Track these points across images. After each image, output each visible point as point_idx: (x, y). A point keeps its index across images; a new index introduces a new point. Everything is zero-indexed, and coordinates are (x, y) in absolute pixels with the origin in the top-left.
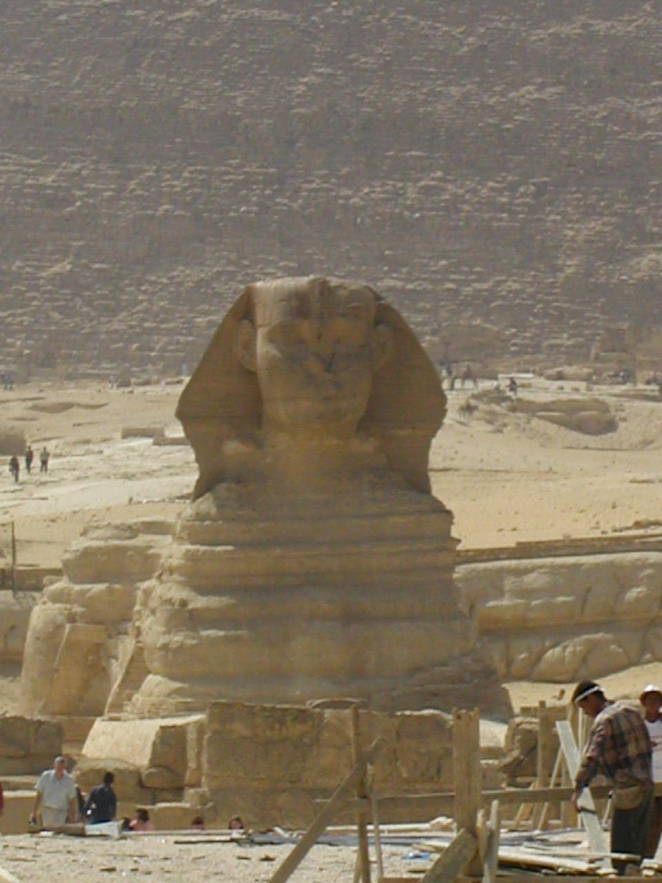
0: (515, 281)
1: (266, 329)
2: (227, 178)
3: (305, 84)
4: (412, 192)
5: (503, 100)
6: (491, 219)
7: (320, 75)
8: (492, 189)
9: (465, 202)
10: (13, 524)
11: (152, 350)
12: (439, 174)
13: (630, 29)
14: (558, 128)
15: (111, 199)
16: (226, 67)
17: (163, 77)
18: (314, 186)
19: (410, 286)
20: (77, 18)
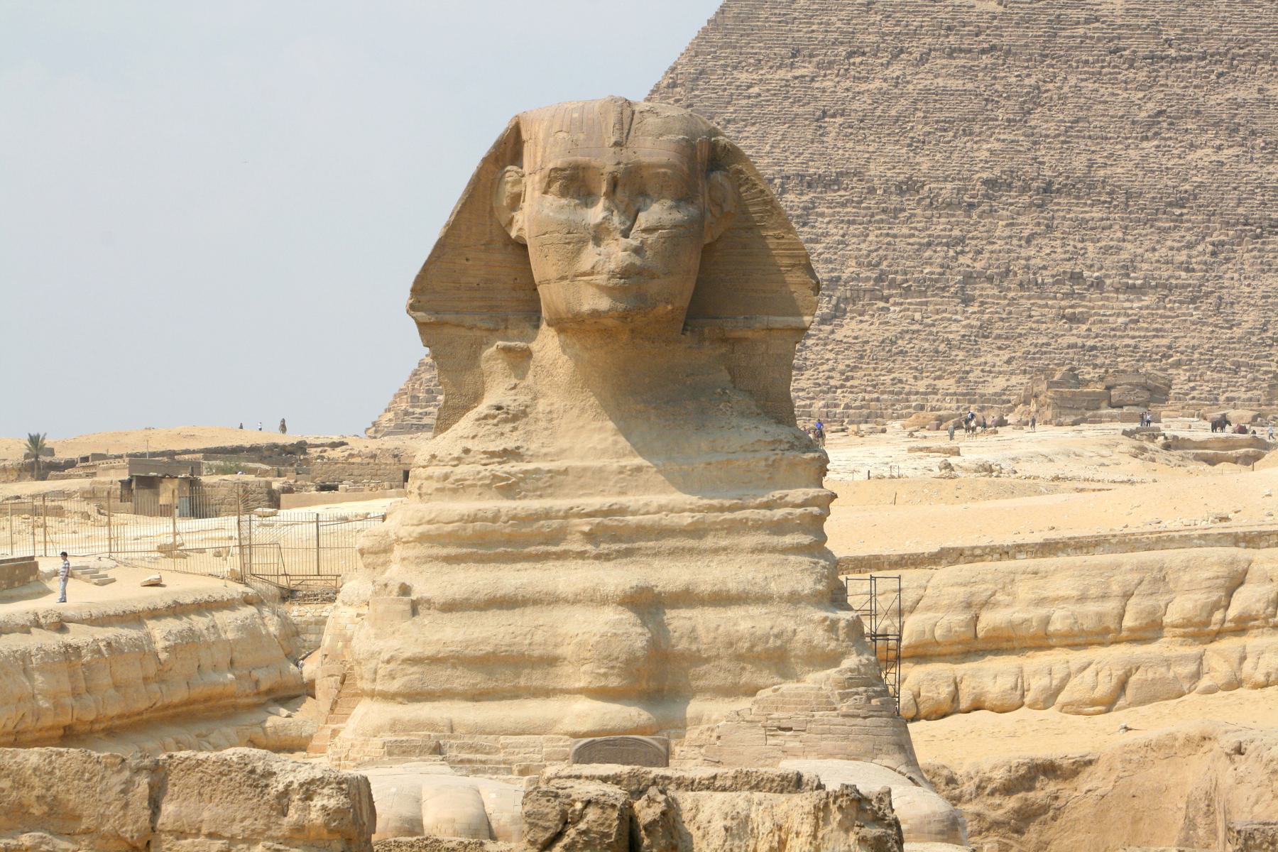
0: (1194, 337)
1: (537, 178)
2: (911, 240)
3: (988, 150)
5: (1181, 162)
6: (1170, 277)
7: (1004, 141)
8: (1172, 249)
11: (836, 406)
12: (1120, 234)
14: (1235, 189)
16: (911, 135)
17: (851, 145)
18: (996, 247)
19: (1090, 343)
20: (768, 90)
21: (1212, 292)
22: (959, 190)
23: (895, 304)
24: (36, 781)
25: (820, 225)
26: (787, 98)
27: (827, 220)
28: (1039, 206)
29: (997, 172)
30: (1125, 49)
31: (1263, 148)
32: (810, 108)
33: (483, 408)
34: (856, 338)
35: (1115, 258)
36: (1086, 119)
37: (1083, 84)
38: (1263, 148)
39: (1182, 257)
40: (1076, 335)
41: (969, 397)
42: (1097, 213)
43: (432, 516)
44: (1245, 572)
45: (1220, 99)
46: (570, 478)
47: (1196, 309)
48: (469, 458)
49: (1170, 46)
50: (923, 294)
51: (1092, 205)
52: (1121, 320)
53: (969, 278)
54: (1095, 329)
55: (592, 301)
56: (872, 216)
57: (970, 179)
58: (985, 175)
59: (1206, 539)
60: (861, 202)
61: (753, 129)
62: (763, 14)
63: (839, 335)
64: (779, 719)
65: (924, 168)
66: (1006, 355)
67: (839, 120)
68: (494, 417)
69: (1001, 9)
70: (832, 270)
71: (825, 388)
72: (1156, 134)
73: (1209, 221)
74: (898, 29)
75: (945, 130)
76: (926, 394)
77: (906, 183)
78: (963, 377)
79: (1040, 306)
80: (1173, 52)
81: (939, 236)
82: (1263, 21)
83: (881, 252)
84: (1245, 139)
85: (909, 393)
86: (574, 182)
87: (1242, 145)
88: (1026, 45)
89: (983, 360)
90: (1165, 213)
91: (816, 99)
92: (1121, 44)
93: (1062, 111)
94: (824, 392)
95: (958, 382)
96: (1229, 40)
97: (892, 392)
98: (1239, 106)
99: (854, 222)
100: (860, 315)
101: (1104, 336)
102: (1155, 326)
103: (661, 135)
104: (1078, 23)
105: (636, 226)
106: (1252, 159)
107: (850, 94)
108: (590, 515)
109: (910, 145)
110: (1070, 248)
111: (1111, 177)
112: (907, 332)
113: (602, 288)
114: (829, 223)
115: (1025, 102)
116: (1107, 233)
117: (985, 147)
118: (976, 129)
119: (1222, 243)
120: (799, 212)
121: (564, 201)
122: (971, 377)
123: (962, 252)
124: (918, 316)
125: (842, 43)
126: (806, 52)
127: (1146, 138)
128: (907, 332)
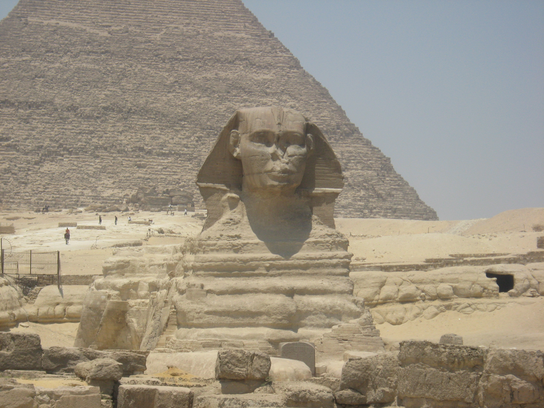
0: (189, 175)
1: (248, 135)
2: (73, 131)
3: (105, 94)
4: (148, 138)
5: (184, 102)
6: (180, 150)
7: (111, 91)
8: (180, 138)
9: (169, 143)
10: (58, 253)
11: (42, 200)
12: (159, 132)
13: (235, 76)
14: (206, 114)
15: (26, 139)
16: (73, 87)
17: (47, 90)
18: (108, 135)
19: (147, 176)
20: (12, 65)
21: (197, 157)
22: (93, 110)
23: (67, 158)
24: (511, 359)
25: (34, 123)
26: (20, 69)
27: (37, 121)
28: (125, 119)
29: (109, 104)
30: (161, 55)
31: (218, 98)
32: (30, 73)
33: (224, 219)
34: (49, 171)
35: (158, 141)
36: (144, 83)
37: (143, 69)
38: (218, 98)
39: (184, 142)
40: (141, 173)
41: (96, 198)
42: (150, 122)
43: (211, 259)
44: (385, 281)
45: (200, 77)
46: (259, 246)
47: (191, 164)
48: (222, 238)
49: (180, 54)
50: (77, 154)
51: (148, 119)
52: (160, 167)
53: (96, 148)
54: (149, 171)
55: (270, 182)
56: (56, 120)
57: (97, 106)
58: (103, 105)
59: (370, 268)
60: (51, 114)
61: (6, 82)
62: (9, 33)
63: (42, 170)
64: (342, 337)
65: (78, 101)
66: (112, 181)
67: (42, 79)
68: (230, 223)
69: (109, 35)
70: (39, 143)
71: (37, 192)
72: (174, 90)
73: (196, 127)
74: (67, 42)
75: (87, 85)
76: (78, 196)
77: (70, 107)
78: (94, 189)
79: (126, 161)
80: (181, 57)
81: (84, 130)
82: (218, 45)
83: (60, 136)
84: (210, 94)
85: (72, 195)
86: (263, 137)
87: (209, 97)
88: (120, 51)
89: (102, 182)
90: (178, 123)
91: (32, 70)
92: (160, 52)
93: (135, 79)
94: (37, 194)
95: (93, 191)
96: (204, 53)
97: (65, 195)
98: (208, 80)
99: (48, 123)
100: (52, 161)
101: (153, 174)
102: (174, 170)
103: (294, 121)
104: (141, 43)
105: (286, 154)
106: (213, 102)
107: (46, 68)
108: (268, 260)
109: (72, 91)
110: (139, 137)
111: (155, 108)
112: (71, 169)
113: (275, 178)
114: (38, 122)
115: (120, 75)
116: (154, 131)
117: (103, 93)
118: (99, 85)
119: (201, 137)
120: (25, 117)
121: (259, 144)
122: (98, 189)
123: (93, 137)
124: (75, 163)
125: (43, 47)
126: (28, 50)
127: (169, 92)
128: (71, 169)
